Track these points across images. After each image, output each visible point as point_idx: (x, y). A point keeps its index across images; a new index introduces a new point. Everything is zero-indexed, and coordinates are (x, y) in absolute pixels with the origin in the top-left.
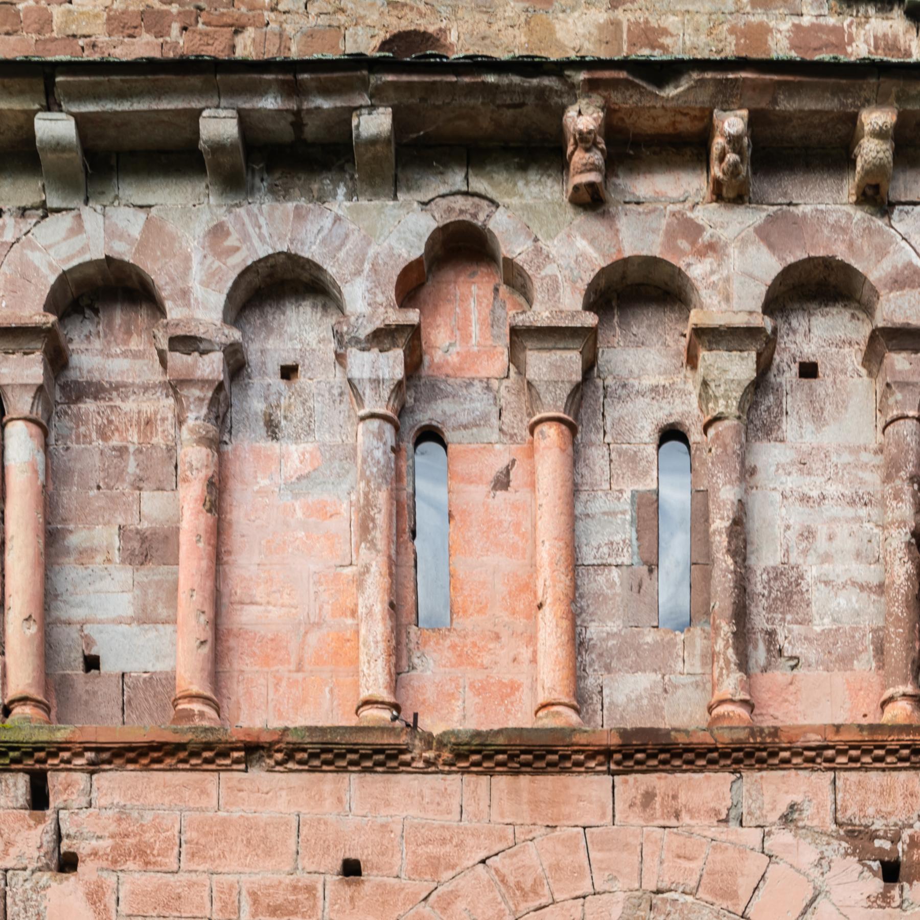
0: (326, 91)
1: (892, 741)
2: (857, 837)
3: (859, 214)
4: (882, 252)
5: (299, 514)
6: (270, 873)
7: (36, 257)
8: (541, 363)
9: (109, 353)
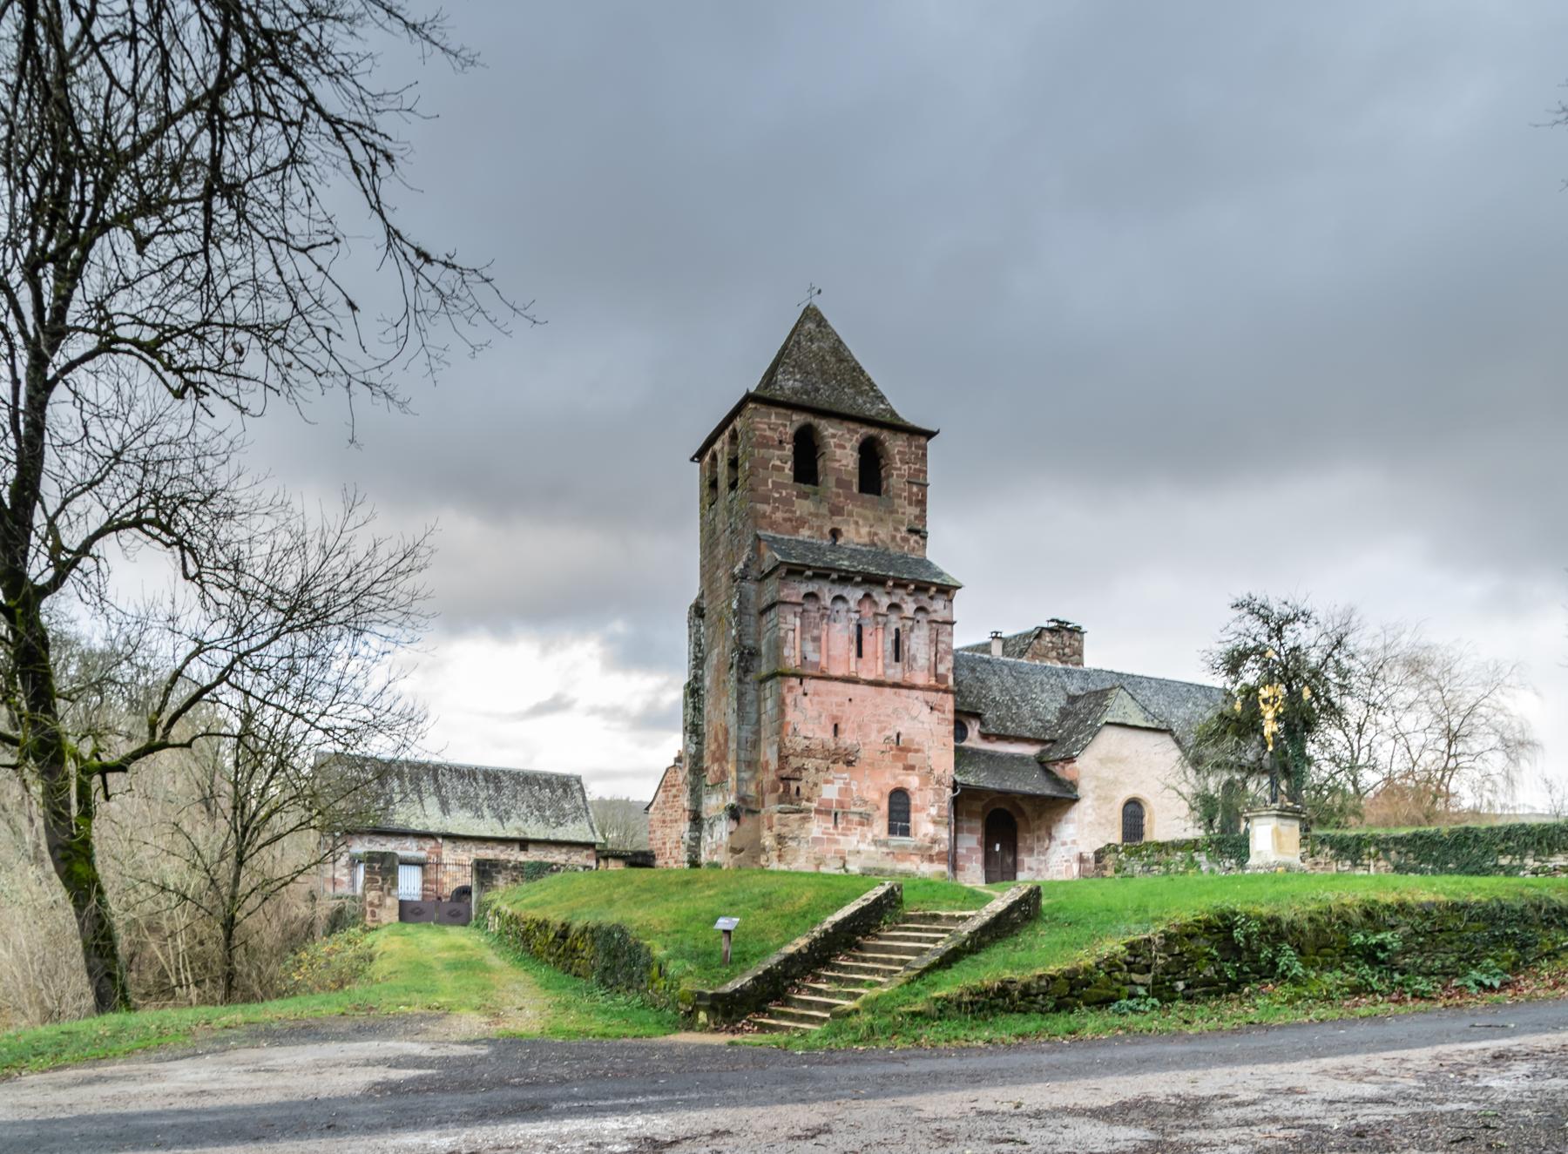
6: (835, 699)
8: (880, 619)
9: (810, 606)
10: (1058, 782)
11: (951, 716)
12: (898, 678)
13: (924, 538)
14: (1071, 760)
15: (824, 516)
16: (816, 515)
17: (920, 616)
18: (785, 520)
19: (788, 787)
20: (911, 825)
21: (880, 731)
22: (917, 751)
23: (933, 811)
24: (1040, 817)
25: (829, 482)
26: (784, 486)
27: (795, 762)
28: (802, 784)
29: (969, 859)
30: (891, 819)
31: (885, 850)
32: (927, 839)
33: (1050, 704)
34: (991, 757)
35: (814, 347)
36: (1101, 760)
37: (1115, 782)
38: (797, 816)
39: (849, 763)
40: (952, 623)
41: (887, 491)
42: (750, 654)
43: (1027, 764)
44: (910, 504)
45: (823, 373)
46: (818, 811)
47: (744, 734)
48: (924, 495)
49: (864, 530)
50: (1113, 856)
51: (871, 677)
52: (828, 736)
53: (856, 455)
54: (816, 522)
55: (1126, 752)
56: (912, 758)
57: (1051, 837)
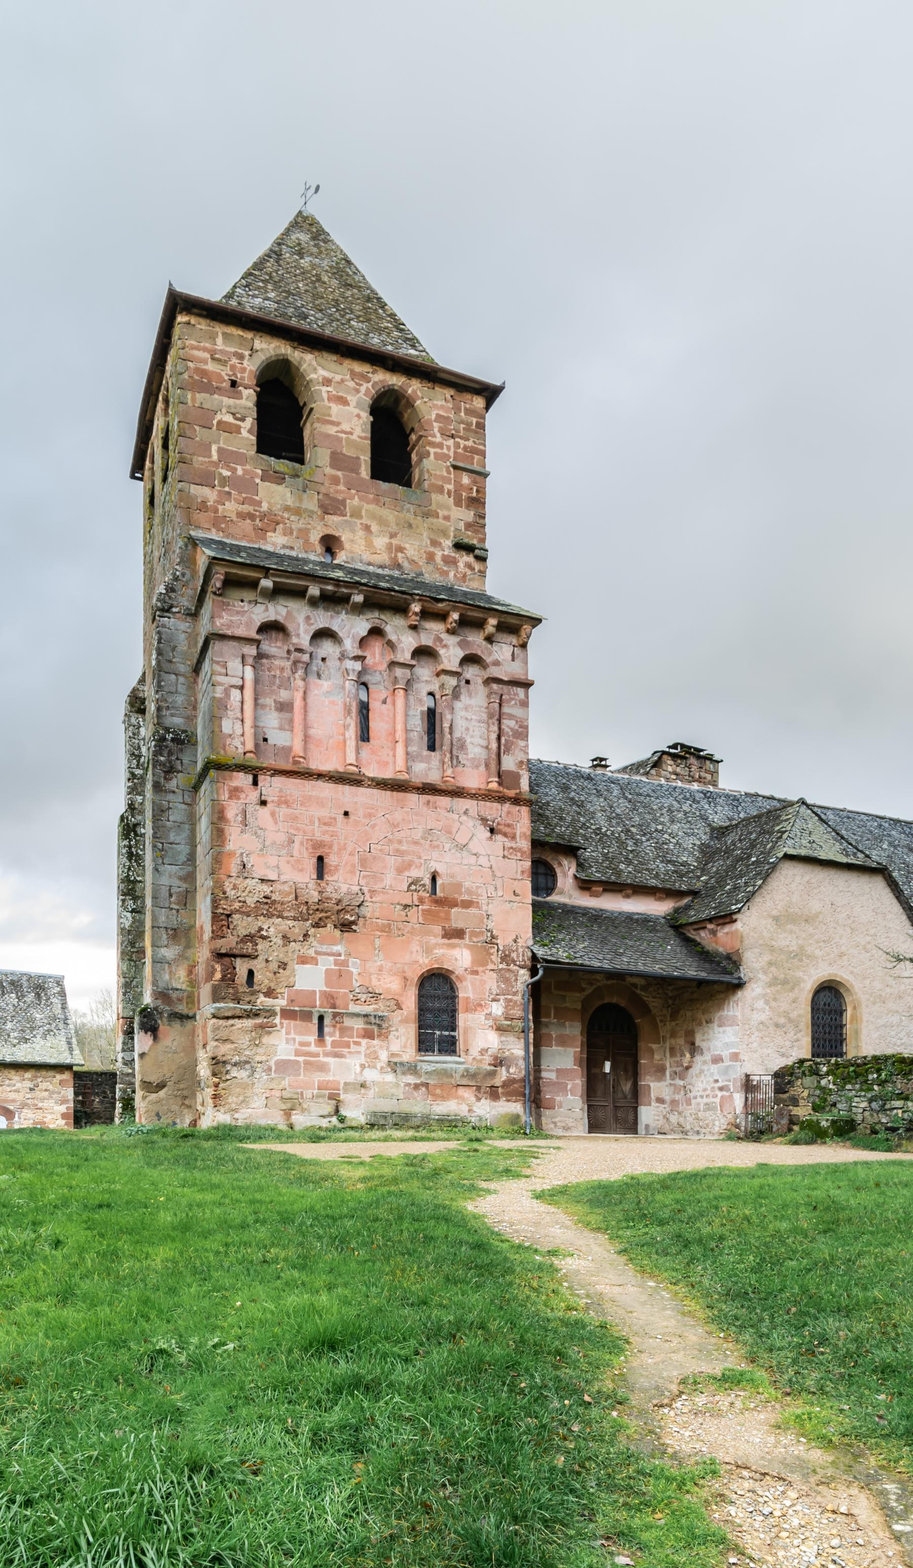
0: (346, 587)
1: (494, 794)
2: (484, 820)
3: (484, 643)
4: (490, 654)
6: (324, 813)
10: (705, 956)
11: (526, 845)
12: (434, 777)
13: (482, 559)
14: (727, 918)
15: (311, 514)
16: (298, 512)
17: (471, 672)
18: (242, 516)
19: (235, 973)
20: (459, 1034)
21: (400, 871)
22: (467, 904)
23: (497, 1009)
24: (674, 1015)
25: (318, 456)
26: (240, 458)
27: (243, 925)
28: (257, 965)
29: (561, 1087)
30: (422, 1025)
31: (411, 1079)
32: (488, 1059)
33: (686, 841)
34: (596, 918)
35: (305, 262)
36: (776, 919)
37: (800, 955)
38: (249, 1023)
39: (346, 927)
40: (527, 685)
41: (421, 482)
42: (176, 740)
43: (654, 930)
45: (316, 296)
46: (287, 1014)
47: (165, 881)
48: (481, 491)
49: (381, 542)
50: (809, 1081)
52: (306, 876)
53: (366, 417)
54: (297, 523)
55: (815, 906)
56: (458, 917)
57: (694, 1049)
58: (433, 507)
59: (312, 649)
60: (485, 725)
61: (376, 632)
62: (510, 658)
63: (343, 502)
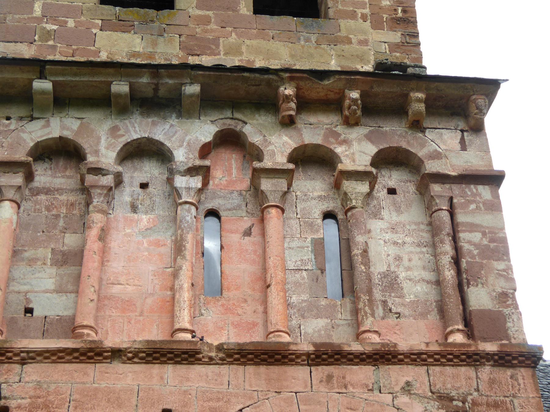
5: (146, 245)
7: (25, 136)
40: (495, 179)
44: (377, 25)
51: (232, 337)
58: (343, 33)
59: (120, 169)
60: (430, 250)
61: (229, 140)
62: (458, 147)
63: (216, 41)
